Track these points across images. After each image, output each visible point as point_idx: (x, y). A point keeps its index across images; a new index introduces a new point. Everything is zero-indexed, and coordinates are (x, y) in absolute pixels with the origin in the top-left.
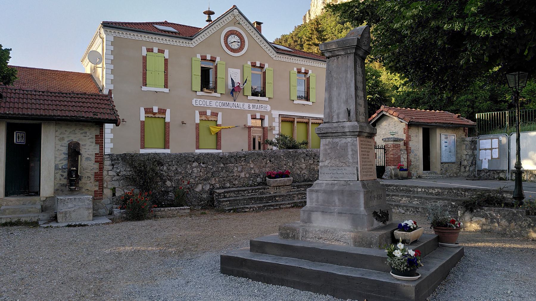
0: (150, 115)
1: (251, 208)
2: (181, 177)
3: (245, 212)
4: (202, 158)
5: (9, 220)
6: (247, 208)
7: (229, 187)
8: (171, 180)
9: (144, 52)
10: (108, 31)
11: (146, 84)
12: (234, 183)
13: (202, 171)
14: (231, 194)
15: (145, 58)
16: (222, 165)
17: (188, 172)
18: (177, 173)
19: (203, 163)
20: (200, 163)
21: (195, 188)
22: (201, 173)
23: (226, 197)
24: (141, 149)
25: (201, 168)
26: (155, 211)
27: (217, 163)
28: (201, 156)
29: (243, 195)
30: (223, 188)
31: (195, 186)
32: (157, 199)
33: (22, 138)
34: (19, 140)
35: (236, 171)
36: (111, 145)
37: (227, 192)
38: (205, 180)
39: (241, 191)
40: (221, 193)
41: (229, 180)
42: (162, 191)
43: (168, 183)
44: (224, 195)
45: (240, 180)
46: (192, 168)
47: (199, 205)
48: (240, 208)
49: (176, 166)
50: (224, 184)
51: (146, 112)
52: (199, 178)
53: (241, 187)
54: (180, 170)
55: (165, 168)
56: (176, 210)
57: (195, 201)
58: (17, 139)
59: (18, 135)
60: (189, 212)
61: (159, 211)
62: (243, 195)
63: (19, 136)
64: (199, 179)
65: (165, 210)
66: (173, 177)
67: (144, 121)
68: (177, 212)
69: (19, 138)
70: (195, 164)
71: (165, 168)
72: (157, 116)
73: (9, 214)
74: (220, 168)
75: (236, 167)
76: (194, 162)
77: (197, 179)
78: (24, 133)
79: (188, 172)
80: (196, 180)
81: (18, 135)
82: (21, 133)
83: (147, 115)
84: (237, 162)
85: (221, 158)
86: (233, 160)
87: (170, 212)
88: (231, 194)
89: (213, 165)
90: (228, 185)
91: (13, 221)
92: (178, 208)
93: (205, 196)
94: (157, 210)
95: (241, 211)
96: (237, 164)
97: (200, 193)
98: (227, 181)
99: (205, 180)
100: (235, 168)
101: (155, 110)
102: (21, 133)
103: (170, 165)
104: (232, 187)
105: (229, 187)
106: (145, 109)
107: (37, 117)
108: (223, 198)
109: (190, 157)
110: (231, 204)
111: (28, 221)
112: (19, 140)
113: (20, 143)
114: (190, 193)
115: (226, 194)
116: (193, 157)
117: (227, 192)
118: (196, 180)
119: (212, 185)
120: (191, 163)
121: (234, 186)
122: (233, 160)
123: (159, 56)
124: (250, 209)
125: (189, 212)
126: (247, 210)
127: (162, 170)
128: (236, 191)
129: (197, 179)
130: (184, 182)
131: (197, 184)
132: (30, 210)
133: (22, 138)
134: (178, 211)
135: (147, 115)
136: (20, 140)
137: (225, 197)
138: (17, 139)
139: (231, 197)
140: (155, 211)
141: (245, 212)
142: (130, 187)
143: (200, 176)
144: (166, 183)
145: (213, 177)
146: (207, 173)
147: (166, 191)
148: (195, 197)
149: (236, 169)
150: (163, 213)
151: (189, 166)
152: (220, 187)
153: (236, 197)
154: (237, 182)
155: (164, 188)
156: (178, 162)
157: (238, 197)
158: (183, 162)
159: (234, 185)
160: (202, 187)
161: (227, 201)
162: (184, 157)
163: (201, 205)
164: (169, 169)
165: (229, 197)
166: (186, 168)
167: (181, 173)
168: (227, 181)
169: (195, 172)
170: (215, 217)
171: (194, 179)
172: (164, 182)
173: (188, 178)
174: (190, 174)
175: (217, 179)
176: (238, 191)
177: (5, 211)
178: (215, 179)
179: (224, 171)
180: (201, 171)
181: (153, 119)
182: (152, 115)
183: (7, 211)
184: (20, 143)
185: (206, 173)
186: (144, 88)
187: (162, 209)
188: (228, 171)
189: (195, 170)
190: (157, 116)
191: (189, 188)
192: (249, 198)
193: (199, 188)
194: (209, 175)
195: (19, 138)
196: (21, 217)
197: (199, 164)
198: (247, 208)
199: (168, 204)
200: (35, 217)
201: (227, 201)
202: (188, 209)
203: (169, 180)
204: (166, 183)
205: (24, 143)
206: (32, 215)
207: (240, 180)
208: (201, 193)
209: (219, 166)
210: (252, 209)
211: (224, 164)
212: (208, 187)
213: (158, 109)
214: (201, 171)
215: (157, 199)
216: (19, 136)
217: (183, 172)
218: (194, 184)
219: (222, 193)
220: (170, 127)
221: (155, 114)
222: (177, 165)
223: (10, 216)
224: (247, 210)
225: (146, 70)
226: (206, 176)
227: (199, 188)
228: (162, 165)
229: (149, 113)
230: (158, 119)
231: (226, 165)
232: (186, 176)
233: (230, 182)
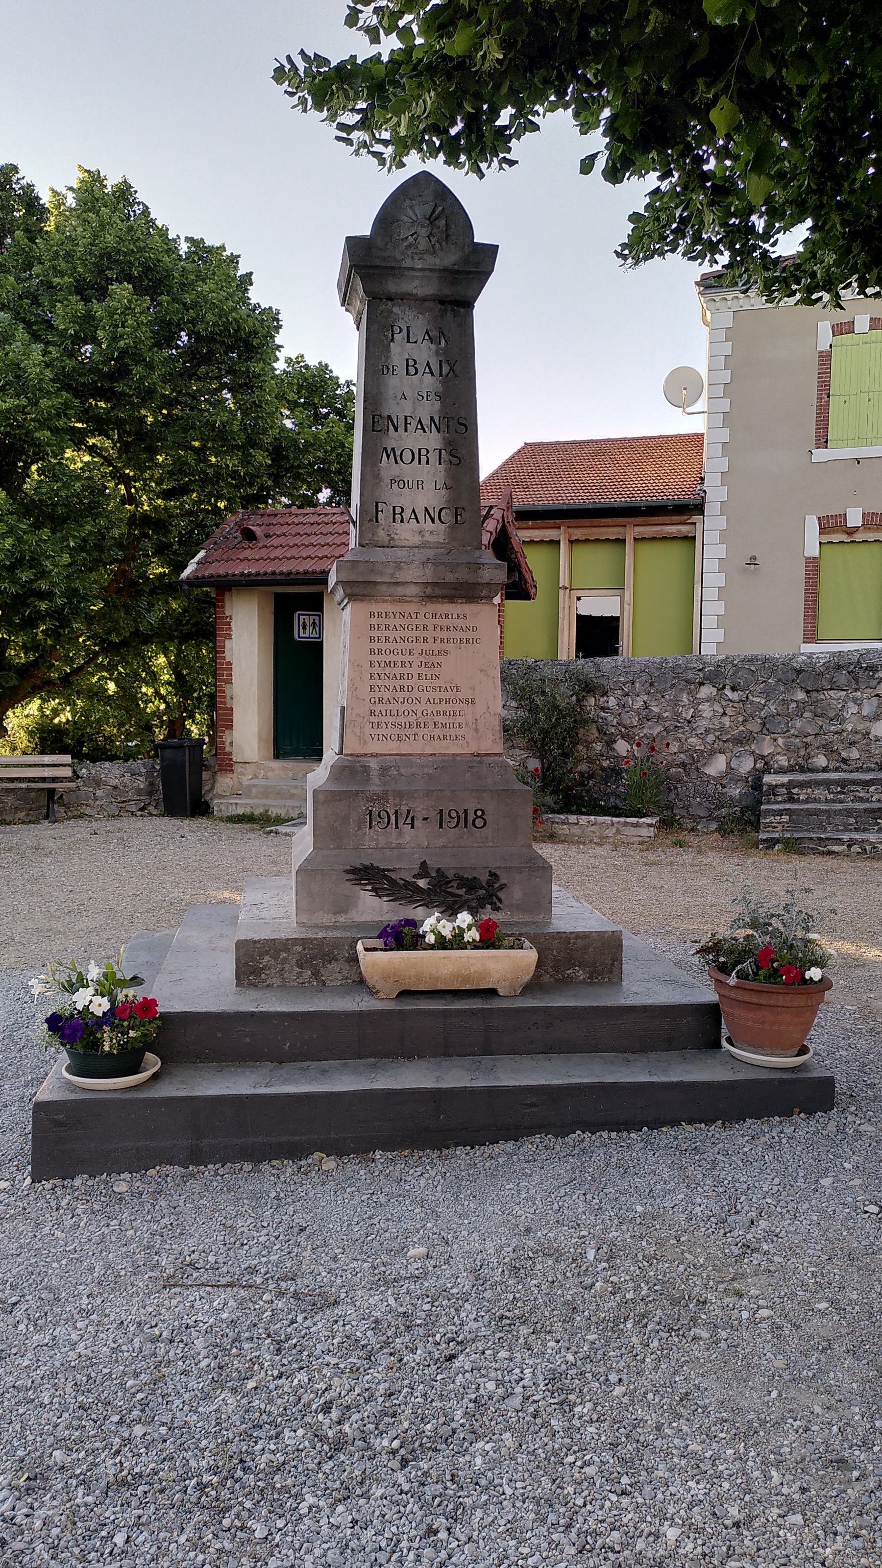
0: (836, 538)
1: (851, 843)
2: (659, 729)
3: (830, 853)
4: (729, 670)
5: (248, 810)
6: (840, 841)
7: (825, 770)
8: (627, 737)
9: (825, 337)
10: (729, 297)
11: (826, 442)
12: (844, 754)
13: (729, 711)
14: (816, 792)
15: (825, 358)
16: (801, 696)
17: (684, 715)
18: (646, 717)
19: (733, 689)
20: (724, 688)
21: (705, 765)
22: (726, 721)
23: (798, 801)
24: (804, 642)
25: (724, 703)
26: (553, 823)
27: (782, 689)
28: (729, 667)
29: (861, 800)
30: (802, 770)
31: (704, 758)
32: (588, 792)
33: (314, 627)
34: (304, 633)
35: (854, 718)
36: (719, 635)
37: (802, 785)
38: (739, 741)
39: (854, 782)
40: (776, 786)
41: (824, 746)
42: (604, 769)
43: (622, 747)
44: (790, 793)
45: (868, 745)
46: (696, 703)
47: (710, 818)
48: (811, 839)
49: (645, 698)
50: (809, 757)
51: (824, 530)
52: (717, 734)
53: (873, 770)
54: (656, 710)
55: (612, 702)
56: (613, 825)
57: (700, 804)
58: (301, 630)
59: (301, 621)
60: (652, 835)
61: (563, 823)
62: (861, 800)
63: (304, 623)
64: (717, 737)
65: (581, 822)
66: (635, 730)
67: (815, 558)
68: (614, 830)
69: (304, 628)
70: (706, 691)
71: (612, 702)
72: (858, 537)
73: (258, 798)
74: (794, 705)
75: (855, 700)
76: (701, 684)
77: (711, 738)
78: (299, 615)
79: (684, 715)
80: (708, 740)
81: (301, 621)
82: (309, 615)
83: (826, 538)
84: (857, 682)
85: (799, 672)
86: (842, 678)
87: (592, 829)
88: (816, 792)
89: (768, 694)
90: (821, 761)
91: (256, 813)
92: (622, 819)
93: (735, 791)
94: (557, 820)
95: (813, 849)
96: (856, 690)
97: (722, 780)
98: (818, 748)
99: (739, 741)
100: (851, 704)
101: (855, 519)
102: (309, 615)
103: (627, 695)
104: (837, 770)
105: (825, 770)
106: (819, 518)
107: (308, 577)
108: (784, 802)
109: (690, 669)
110: (795, 824)
111: (283, 816)
112: (304, 633)
113: (309, 638)
114: (685, 778)
115: (795, 791)
116: (700, 670)
117: (802, 785)
118: (708, 740)
119: (763, 757)
120: (692, 687)
121: (844, 767)
122: (842, 678)
123: (874, 339)
124: (849, 846)
125: (652, 835)
126: (836, 848)
127: (603, 709)
128: (837, 783)
129: (711, 738)
130: (668, 744)
131: (712, 753)
132: (293, 791)
133: (314, 627)
134: (618, 830)
135: (826, 538)
136: (307, 631)
137: (791, 799)
138: (301, 630)
139: (815, 800)
140: (553, 823)
141: (830, 853)
142: (518, 751)
143: (722, 729)
144: (615, 746)
145: (765, 731)
146: (745, 721)
147: (613, 770)
148: (704, 794)
149: (853, 708)
150: (576, 830)
151: (685, 695)
152: (792, 766)
153: (833, 801)
154: (855, 754)
155: (608, 758)
156: (651, 684)
157: (841, 802)
158: (669, 685)
159: (844, 761)
160: (728, 764)
161: (780, 813)
162: (673, 669)
163: (717, 819)
164: (624, 706)
165: (806, 801)
166: (676, 702)
167: (659, 717)
168: (818, 748)
169: (707, 714)
170: (652, 857)
171: (702, 737)
172: (610, 743)
173: (683, 733)
174: (689, 722)
175: (780, 741)
176: (843, 783)
177: (251, 791)
178: (775, 740)
179: (807, 714)
180: (724, 714)
181: (847, 547)
182: (844, 538)
183: (254, 790)
184: (309, 638)
185: (741, 719)
186: (820, 455)
187: (573, 818)
188: (821, 716)
189: (706, 710)
190: (858, 537)
191: (683, 765)
192: (865, 810)
193: (717, 766)
194: (754, 726)
195: (304, 628)
196: (270, 806)
197: (718, 690)
198: (840, 841)
199: (616, 807)
200: (293, 808)
201: (780, 813)
202: (650, 825)
203: (623, 737)
204: (615, 746)
205: (299, 637)
206: (289, 803)
207: (868, 745)
208: (724, 782)
209: (788, 697)
210: (856, 848)
211: (808, 692)
212: (746, 765)
213: (864, 514)
214: (724, 714)
215: (588, 792)
216: (304, 623)
217: (665, 715)
218: (703, 751)
219: (782, 785)
220: (804, 569)
221: (851, 531)
222: (648, 693)
223: (264, 801)
224: (836, 848)
225: (828, 397)
226: (741, 728)
227: (717, 766)
228: (605, 694)
229: (833, 532)
230: (863, 547)
231: (815, 694)
232: (676, 727)
233: (828, 749)
